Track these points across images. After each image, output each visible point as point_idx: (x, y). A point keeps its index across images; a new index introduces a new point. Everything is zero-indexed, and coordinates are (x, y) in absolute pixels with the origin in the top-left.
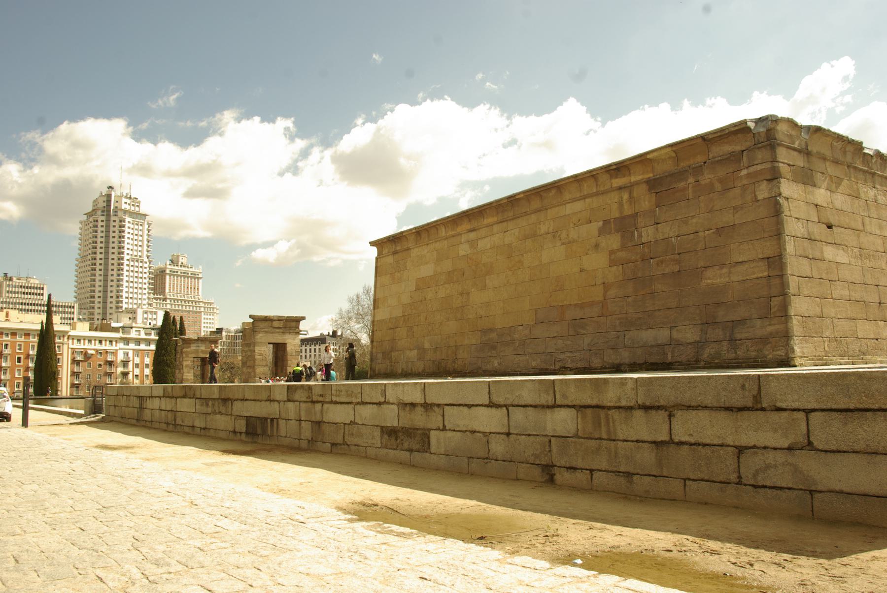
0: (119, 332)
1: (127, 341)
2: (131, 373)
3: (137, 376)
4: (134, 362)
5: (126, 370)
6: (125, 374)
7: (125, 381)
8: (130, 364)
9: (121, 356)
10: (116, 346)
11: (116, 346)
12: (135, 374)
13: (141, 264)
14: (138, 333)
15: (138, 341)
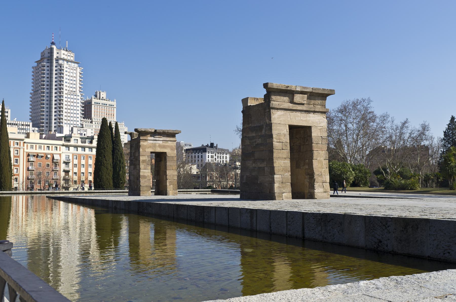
0: (62, 140)
1: (68, 147)
2: (71, 171)
3: (76, 173)
4: (73, 162)
5: (67, 169)
6: (67, 172)
7: (67, 177)
8: (71, 164)
9: (63, 159)
10: (60, 150)
11: (60, 150)
12: (74, 171)
13: (75, 97)
14: (76, 141)
15: (76, 147)
